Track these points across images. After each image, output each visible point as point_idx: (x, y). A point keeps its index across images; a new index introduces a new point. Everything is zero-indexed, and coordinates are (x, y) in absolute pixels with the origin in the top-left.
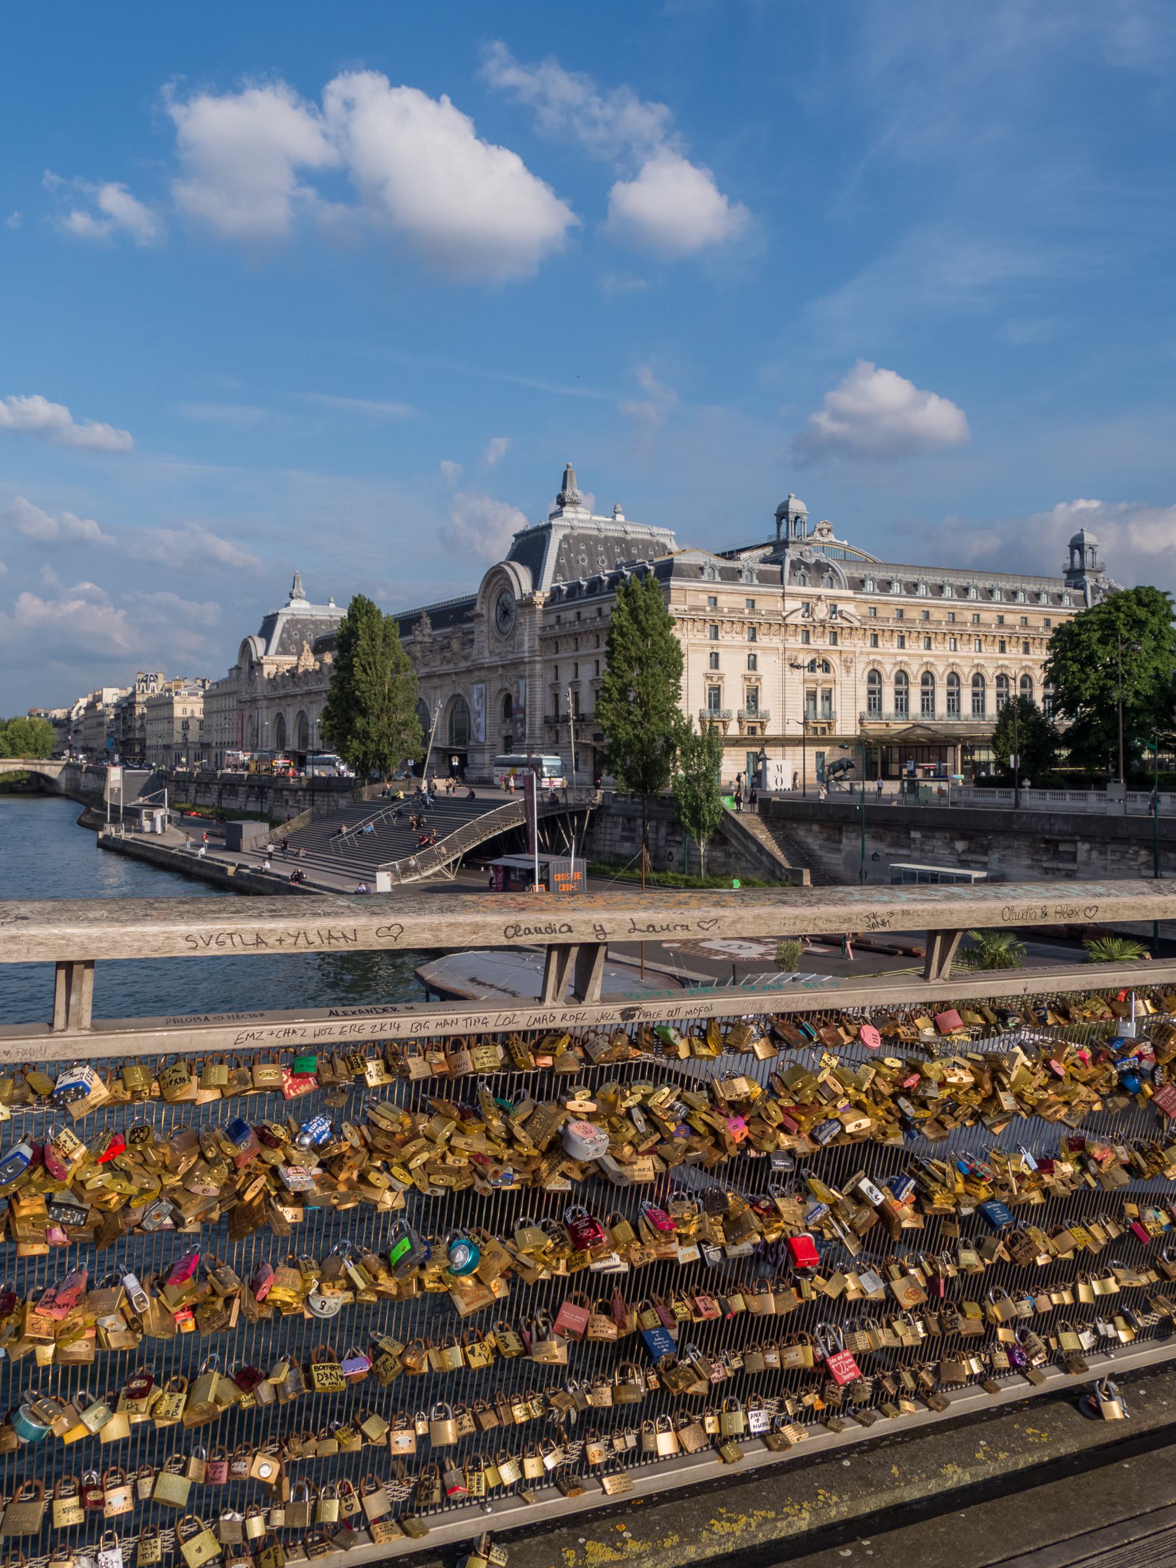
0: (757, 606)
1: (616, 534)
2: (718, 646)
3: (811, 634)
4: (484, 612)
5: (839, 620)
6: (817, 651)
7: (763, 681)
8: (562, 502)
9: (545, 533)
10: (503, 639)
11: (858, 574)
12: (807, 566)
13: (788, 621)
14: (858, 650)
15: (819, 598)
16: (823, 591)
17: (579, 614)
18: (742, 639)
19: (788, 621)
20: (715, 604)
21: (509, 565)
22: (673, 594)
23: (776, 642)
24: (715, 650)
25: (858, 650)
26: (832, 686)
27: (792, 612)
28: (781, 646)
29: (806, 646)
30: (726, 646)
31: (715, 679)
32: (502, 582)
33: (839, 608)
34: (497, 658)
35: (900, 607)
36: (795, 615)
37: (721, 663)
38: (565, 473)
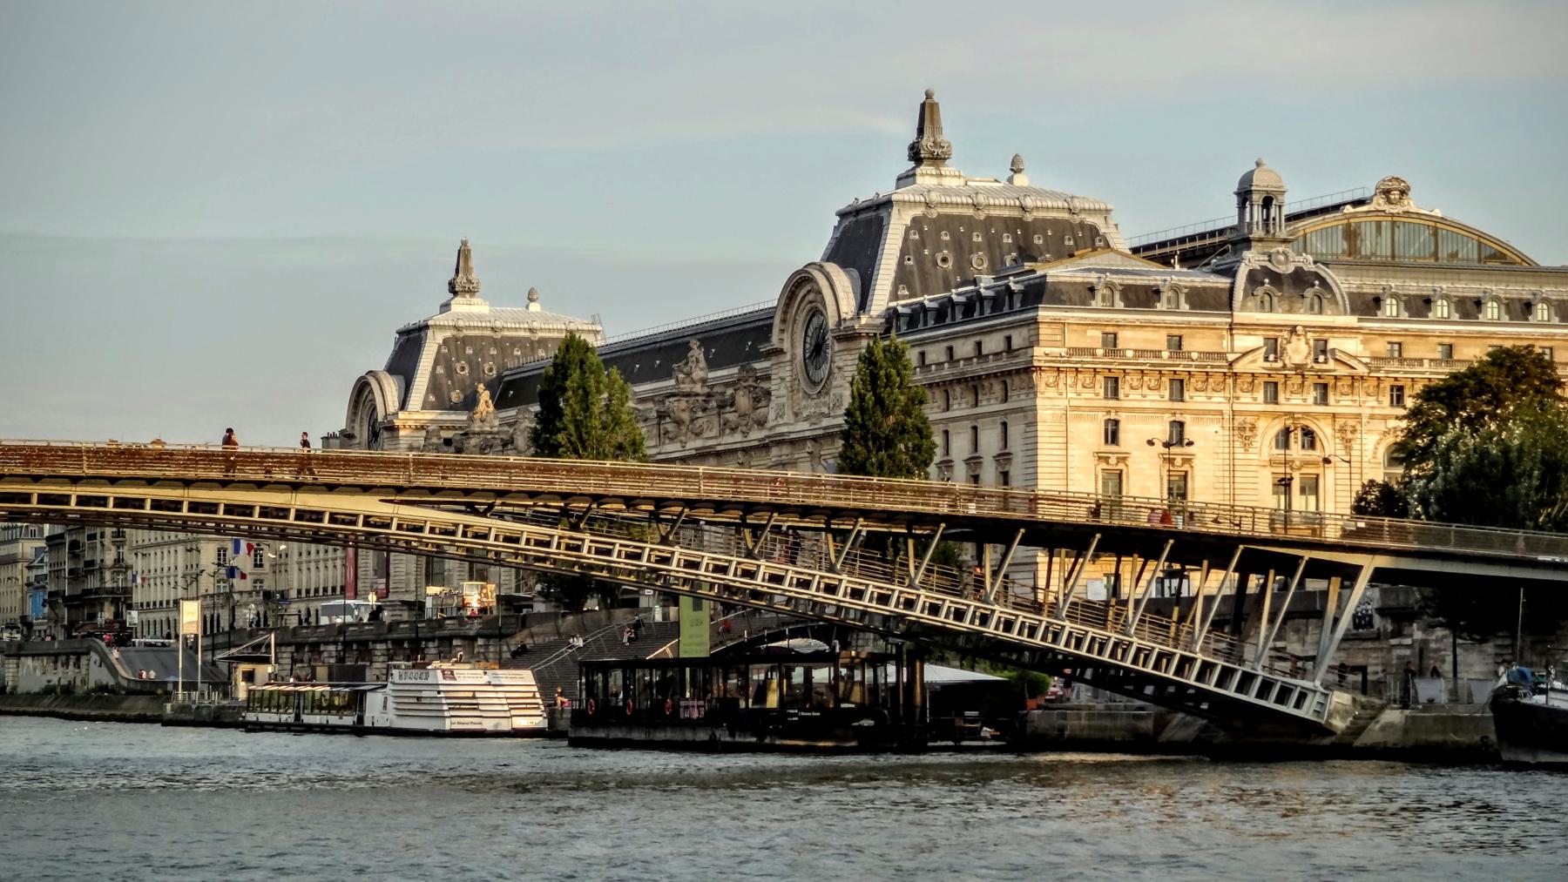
0: (1186, 346)
1: (1006, 213)
2: (1117, 410)
3: (1280, 387)
4: (786, 346)
5: (1331, 364)
6: (1291, 414)
7: (1195, 462)
8: (916, 155)
9: (883, 213)
10: (814, 392)
11: (1369, 284)
12: (1276, 278)
13: (1238, 368)
14: (1366, 412)
15: (1293, 330)
16: (1301, 318)
17: (923, 354)
18: (1158, 398)
19: (1238, 368)
20: (1115, 345)
21: (821, 268)
22: (1044, 331)
23: (1218, 401)
25: (1366, 412)
26: (1319, 471)
27: (1244, 354)
28: (1226, 408)
29: (1271, 407)
30: (1132, 410)
31: (1113, 460)
32: (811, 297)
33: (1331, 345)
34: (805, 426)
35: (1447, 341)
36: (1249, 357)
37: (1122, 436)
38: (923, 106)
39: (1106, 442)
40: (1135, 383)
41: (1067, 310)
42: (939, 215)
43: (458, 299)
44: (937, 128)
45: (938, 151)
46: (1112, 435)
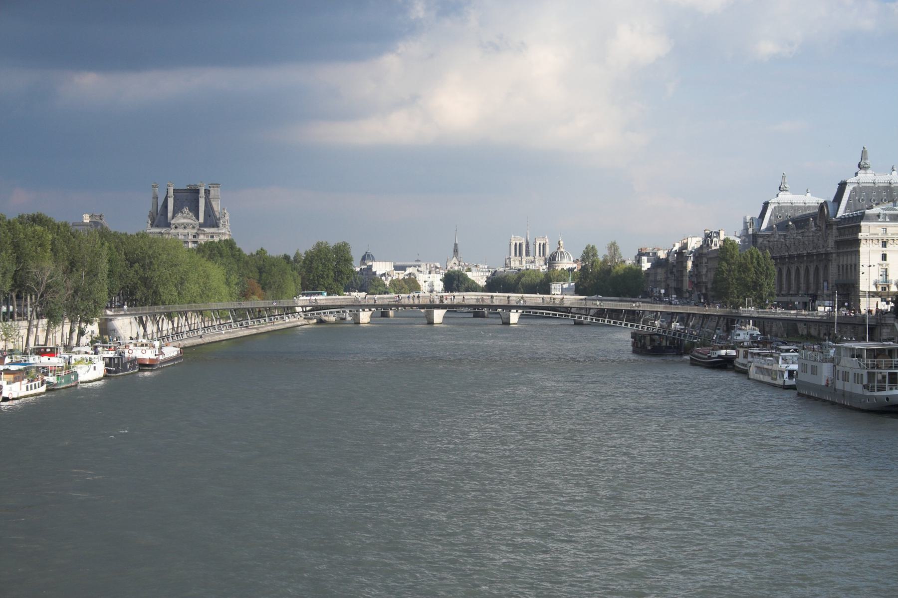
1: (885, 185)
2: (886, 251)
24: (884, 253)
37: (888, 258)
39: (882, 260)
40: (892, 243)
41: (870, 222)
42: (862, 186)
43: (782, 193)
44: (866, 159)
45: (866, 166)
46: (884, 257)
